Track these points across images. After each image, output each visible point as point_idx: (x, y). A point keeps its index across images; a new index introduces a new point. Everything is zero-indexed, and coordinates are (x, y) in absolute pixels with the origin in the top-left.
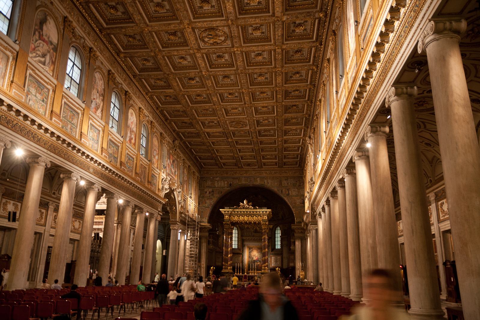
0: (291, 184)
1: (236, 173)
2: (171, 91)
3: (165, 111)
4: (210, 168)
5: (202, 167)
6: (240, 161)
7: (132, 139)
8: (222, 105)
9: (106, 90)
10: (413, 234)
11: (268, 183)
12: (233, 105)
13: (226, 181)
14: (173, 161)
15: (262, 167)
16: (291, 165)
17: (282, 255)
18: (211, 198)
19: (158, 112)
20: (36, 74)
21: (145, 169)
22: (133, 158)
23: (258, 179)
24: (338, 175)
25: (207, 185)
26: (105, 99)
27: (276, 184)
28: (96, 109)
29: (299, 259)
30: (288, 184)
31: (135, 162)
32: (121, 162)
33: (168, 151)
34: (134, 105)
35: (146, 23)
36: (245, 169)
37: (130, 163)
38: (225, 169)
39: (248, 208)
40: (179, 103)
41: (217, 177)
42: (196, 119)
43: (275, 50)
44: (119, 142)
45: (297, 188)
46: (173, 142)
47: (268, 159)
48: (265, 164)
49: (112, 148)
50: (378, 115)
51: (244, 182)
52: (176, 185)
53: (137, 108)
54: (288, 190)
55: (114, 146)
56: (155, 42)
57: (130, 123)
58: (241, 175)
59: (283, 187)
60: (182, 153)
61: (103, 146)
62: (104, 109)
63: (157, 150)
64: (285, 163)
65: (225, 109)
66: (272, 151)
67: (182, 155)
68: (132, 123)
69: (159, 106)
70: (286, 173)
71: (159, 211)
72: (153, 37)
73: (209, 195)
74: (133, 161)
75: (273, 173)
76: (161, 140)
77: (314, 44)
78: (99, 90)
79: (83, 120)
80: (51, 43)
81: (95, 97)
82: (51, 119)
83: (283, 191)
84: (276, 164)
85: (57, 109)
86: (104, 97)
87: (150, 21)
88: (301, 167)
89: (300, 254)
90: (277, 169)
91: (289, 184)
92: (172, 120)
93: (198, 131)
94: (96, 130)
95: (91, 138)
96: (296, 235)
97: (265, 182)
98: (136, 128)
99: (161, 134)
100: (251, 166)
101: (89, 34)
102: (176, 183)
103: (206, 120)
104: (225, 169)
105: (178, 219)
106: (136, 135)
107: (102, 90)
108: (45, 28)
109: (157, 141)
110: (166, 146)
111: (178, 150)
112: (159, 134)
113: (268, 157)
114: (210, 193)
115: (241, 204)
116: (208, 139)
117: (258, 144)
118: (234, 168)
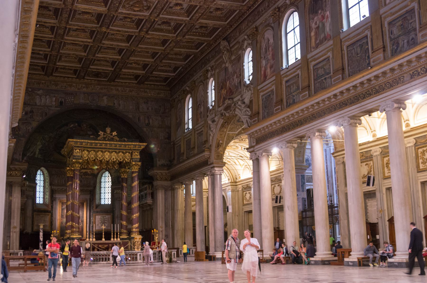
0: (152, 109)
11: (120, 106)
13: (55, 96)
16: (157, 81)
23: (105, 98)
27: (131, 107)
30: (148, 109)
39: (112, 140)
41: (39, 90)
70: (146, 92)
75: (127, 91)
83: (141, 118)
89: (164, 211)
91: (150, 108)
96: (155, 183)
97: (114, 104)
100: (98, 77)
115: (101, 133)
118: (68, 77)
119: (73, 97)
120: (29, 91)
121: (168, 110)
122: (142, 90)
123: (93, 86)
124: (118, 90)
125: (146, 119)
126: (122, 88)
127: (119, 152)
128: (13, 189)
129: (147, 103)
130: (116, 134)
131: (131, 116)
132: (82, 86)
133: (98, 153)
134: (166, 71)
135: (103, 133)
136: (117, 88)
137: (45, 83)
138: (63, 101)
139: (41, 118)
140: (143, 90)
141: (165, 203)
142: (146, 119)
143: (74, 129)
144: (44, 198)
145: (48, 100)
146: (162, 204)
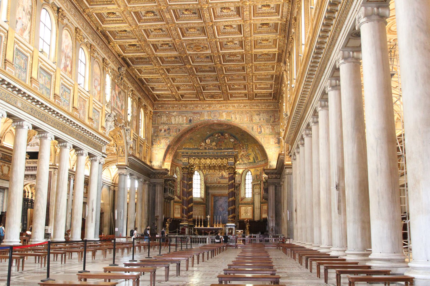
0: (264, 119)
1: (197, 107)
2: (115, 7)
3: (107, 32)
4: (165, 101)
5: (155, 100)
6: (202, 93)
7: (68, 66)
8: (177, 24)
9: (34, 6)
10: (378, 173)
11: (236, 118)
12: (190, 23)
13: (185, 116)
14: (120, 93)
15: (229, 100)
16: (264, 96)
17: (254, 206)
18: (167, 138)
21: (84, 103)
22: (70, 90)
23: (224, 114)
24: (311, 108)
25: (162, 122)
26: (33, 18)
27: (246, 119)
28: (22, 31)
29: (273, 210)
33: (113, 80)
34: (69, 24)
36: (208, 102)
37: (65, 95)
38: (183, 102)
39: (211, 149)
41: (174, 112)
42: (145, 41)
44: (51, 70)
45: (271, 125)
46: (119, 68)
49: (44, 78)
50: (350, 39)
51: (206, 117)
52: (123, 121)
54: (260, 127)
55: (45, 75)
57: (65, 47)
58: (203, 109)
59: (254, 123)
60: (131, 82)
61: (33, 76)
62: (32, 30)
63: (99, 80)
64: (256, 94)
65: (180, 29)
66: (241, 80)
67: (129, 85)
68: (67, 46)
70: (258, 106)
71: (103, 153)
73: (164, 134)
74: (70, 93)
75: (242, 107)
76: (103, 67)
78: (26, 7)
79: (7, 45)
81: (21, 16)
83: (254, 128)
84: (246, 95)
86: (31, 15)
88: (276, 99)
89: (274, 204)
90: (247, 101)
91: (262, 119)
92: (116, 42)
93: (148, 56)
94: (23, 56)
95: (17, 66)
97: (232, 118)
98: (73, 52)
99: (103, 59)
100: (215, 98)
102: (124, 119)
103: (159, 41)
104: (183, 102)
106: (72, 62)
107: (29, 7)
109: (98, 68)
110: (110, 74)
111: (125, 79)
113: (236, 86)
114: (165, 131)
115: (203, 144)
116: (161, 65)
117: (223, 71)
119: (199, 116)
120: (167, 114)
121: (277, 119)
122: (254, 104)
123: (214, 105)
124: (234, 106)
125: (259, 128)
126: (238, 105)
127: (218, 158)
128: (157, 188)
129: (259, 115)
130: (215, 144)
131: (246, 127)
132: (205, 106)
133: (201, 160)
134: (265, 89)
135: (204, 144)
136: (234, 105)
137: (178, 106)
138: (192, 119)
139: (175, 134)
140: (255, 104)
141: (275, 197)
142: (259, 128)
143: (219, 138)
144: (201, 193)
145: (180, 119)
146: (273, 198)
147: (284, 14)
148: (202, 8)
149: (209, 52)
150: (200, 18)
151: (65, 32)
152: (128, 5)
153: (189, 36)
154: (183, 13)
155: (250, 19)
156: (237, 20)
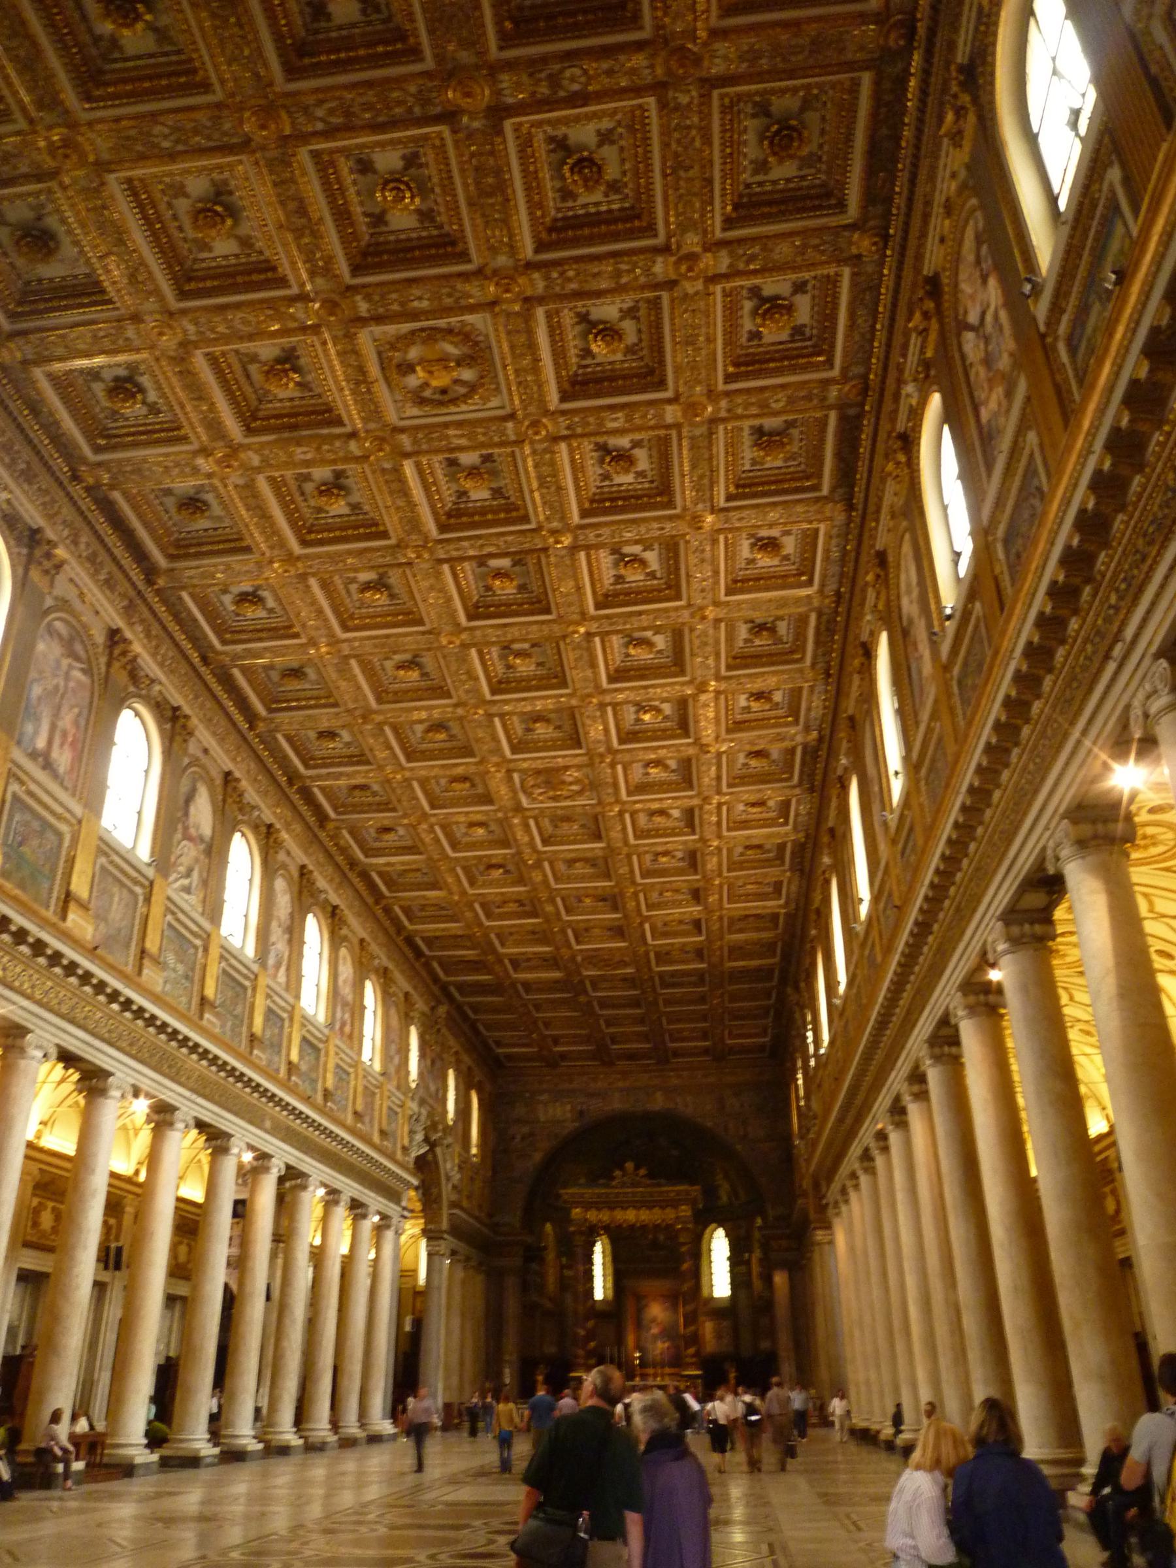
14: (433, 1062)
19: (400, 940)
20: (178, 920)
22: (348, 1074)
31: (353, 1083)
32: (326, 1090)
35: (400, 765)
39: (638, 1185)
40: (453, 919)
42: (494, 951)
43: (701, 808)
46: (433, 1009)
47: (683, 1040)
48: (676, 1054)
53: (356, 941)
56: (417, 799)
67: (452, 1042)
68: (345, 982)
69: (404, 927)
71: (404, 1209)
72: (413, 789)
77: (797, 791)
80: (202, 839)
82: (201, 1017)
84: (706, 1051)
85: (210, 992)
87: (409, 759)
99: (407, 994)
101: (266, 793)
105: (445, 1225)
108: (192, 810)
111: (444, 1030)
112: (401, 995)
114: (523, 1138)
115: (618, 1173)
131: (709, 1124)
134: (750, 1036)
147: (793, 896)
148: (622, 894)
149: (630, 970)
150: (615, 909)
151: (343, 952)
152: (471, 892)
153: (588, 943)
154: (580, 901)
155: (721, 908)
156: (695, 910)
